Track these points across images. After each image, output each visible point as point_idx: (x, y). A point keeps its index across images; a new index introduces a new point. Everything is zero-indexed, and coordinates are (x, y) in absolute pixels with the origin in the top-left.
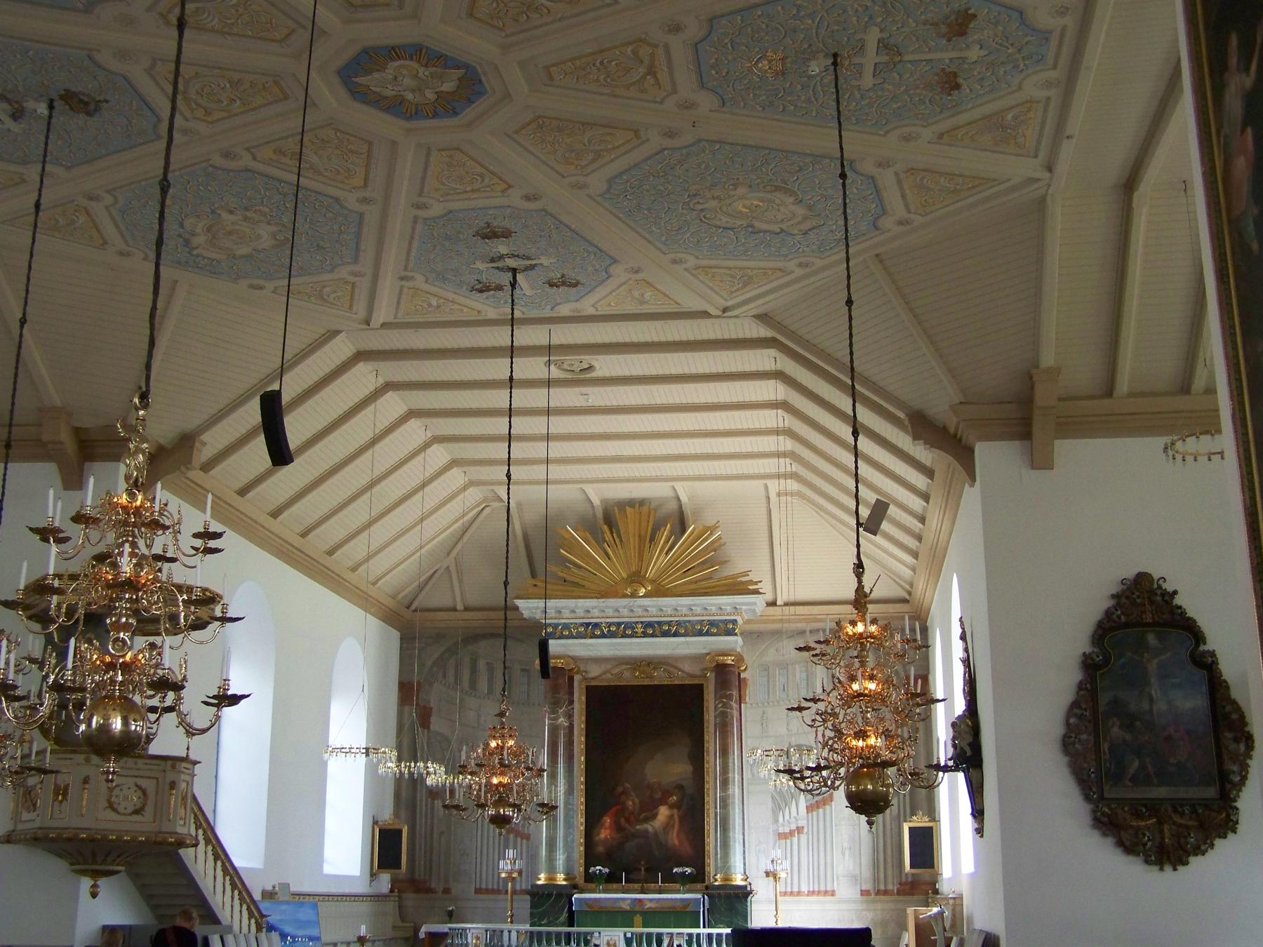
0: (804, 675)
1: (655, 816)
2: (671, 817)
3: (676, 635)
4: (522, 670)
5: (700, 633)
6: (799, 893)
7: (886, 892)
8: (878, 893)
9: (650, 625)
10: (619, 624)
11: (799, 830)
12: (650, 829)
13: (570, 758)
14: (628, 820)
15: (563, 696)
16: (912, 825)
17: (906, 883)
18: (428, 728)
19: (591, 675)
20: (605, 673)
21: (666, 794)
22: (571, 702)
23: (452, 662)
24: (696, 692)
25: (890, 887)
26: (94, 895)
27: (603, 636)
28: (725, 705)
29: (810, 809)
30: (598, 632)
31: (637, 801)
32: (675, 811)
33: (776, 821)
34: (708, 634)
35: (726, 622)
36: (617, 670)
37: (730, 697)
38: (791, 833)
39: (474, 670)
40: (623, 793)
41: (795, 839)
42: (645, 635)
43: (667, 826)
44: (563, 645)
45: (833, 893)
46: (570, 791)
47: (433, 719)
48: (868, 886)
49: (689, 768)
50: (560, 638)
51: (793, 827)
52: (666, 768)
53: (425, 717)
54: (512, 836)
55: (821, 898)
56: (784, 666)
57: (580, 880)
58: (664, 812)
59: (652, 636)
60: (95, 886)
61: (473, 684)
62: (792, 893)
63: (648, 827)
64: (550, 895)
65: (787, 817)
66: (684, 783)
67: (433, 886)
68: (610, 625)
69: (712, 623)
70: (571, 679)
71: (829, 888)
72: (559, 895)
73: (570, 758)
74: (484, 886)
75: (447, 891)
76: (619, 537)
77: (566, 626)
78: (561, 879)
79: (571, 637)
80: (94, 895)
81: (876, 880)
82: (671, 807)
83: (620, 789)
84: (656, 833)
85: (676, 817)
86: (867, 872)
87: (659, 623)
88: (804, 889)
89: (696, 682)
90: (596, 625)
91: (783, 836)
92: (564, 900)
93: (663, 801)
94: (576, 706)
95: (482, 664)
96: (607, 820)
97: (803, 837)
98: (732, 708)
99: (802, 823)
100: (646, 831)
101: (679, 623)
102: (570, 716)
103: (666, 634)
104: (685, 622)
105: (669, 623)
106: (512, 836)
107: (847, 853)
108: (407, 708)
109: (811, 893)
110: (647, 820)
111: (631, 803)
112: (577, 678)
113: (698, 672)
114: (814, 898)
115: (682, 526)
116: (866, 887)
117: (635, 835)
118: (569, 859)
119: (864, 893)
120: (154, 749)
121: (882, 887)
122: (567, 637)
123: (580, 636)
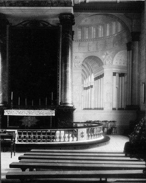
6: (91, 109)
11: (92, 86)
20: (19, 24)
25: (123, 107)
29: (96, 79)
33: (83, 83)
36: (24, 23)
38: (88, 88)
41: (90, 90)
45: (102, 109)
51: (89, 86)
56: (88, 27)
62: (88, 109)
65: (87, 82)
71: (101, 107)
81: (118, 104)
97: (93, 89)
98: (69, 37)
109: (95, 109)
112: (8, 26)
116: (115, 106)
121: (120, 107)
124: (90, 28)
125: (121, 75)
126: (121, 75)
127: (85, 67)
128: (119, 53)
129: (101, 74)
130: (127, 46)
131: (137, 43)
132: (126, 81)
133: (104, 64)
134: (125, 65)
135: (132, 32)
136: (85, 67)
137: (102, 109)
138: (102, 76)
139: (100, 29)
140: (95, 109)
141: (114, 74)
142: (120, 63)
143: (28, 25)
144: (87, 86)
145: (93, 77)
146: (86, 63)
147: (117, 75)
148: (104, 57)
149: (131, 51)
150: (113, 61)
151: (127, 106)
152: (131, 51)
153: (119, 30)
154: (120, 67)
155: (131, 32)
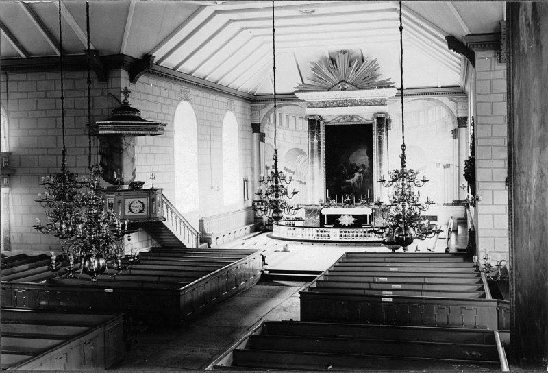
13: (319, 153)
19: (326, 121)
22: (319, 132)
24: (367, 129)
26: (129, 240)
28: (381, 134)
37: (382, 131)
47: (266, 138)
52: (360, 158)
58: (357, 175)
60: (129, 236)
63: (351, 181)
66: (365, 163)
70: (319, 123)
73: (319, 153)
76: (336, 65)
80: (129, 240)
82: (360, 173)
84: (354, 184)
89: (369, 123)
94: (321, 133)
95: (284, 116)
102: (319, 137)
110: (350, 178)
112: (321, 122)
113: (370, 119)
115: (363, 61)
120: (144, 187)
126: (447, 166)
135: (458, 118)
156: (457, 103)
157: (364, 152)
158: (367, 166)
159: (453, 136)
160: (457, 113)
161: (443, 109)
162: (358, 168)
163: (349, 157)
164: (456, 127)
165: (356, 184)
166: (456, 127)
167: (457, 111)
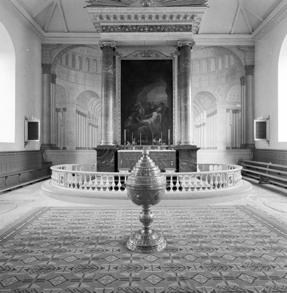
0: (206, 64)
1: (151, 116)
2: (158, 116)
3: (163, 31)
4: (94, 60)
5: (175, 31)
7: (236, 148)
8: (233, 148)
9: (152, 26)
10: (137, 26)
11: (204, 124)
12: (149, 122)
14: (140, 118)
15: (111, 59)
16: (257, 121)
17: (243, 145)
18: (55, 83)
19: (123, 56)
20: (129, 55)
21: (156, 107)
22: (114, 67)
23: (65, 55)
25: (237, 146)
27: (129, 31)
29: (208, 116)
30: (127, 30)
31: (144, 110)
32: (160, 114)
34: (179, 31)
35: (187, 26)
38: (201, 125)
39: (74, 60)
40: (136, 107)
41: (202, 128)
42: (149, 31)
43: (157, 120)
44: (110, 36)
45: (216, 148)
46: (115, 105)
47: (57, 79)
48: (229, 146)
49: (167, 96)
50: (109, 32)
52: (158, 96)
53: (53, 79)
54: (90, 127)
55: (212, 150)
57: (119, 144)
58: (155, 114)
59: (152, 31)
61: (74, 66)
63: (149, 121)
64: (106, 150)
66: (164, 102)
67: (59, 147)
68: (132, 26)
69: (180, 26)
70: (114, 57)
71: (215, 146)
72: (110, 150)
74: (80, 146)
75: (64, 148)
77: (112, 27)
78: (111, 144)
79: (114, 31)
81: (232, 143)
82: (158, 112)
83: (136, 105)
84: (152, 124)
85: (160, 117)
86: (229, 140)
87: (156, 26)
88: (205, 147)
89: (170, 59)
90: (126, 26)
91: (197, 126)
92: (113, 153)
93: (154, 110)
95: (77, 58)
96: (131, 118)
97: (205, 127)
99: (204, 122)
100: (148, 123)
101: (165, 26)
103: (159, 31)
104: (168, 26)
105: (161, 26)
106: (90, 127)
107: (222, 133)
108: (45, 75)
109: (208, 148)
110: (147, 118)
111: (141, 110)
112: (117, 57)
113: (170, 55)
114: (209, 150)
117: (143, 124)
118: (114, 134)
119: (227, 148)
122: (113, 32)
123: (118, 31)
124: (201, 61)
125: (235, 111)
126: (235, 111)
127: (197, 104)
128: (232, 88)
129: (214, 111)
130: (241, 80)
131: (250, 77)
132: (240, 117)
133: (217, 99)
134: (240, 101)
135: (246, 66)
136: (197, 104)
137: (216, 148)
138: (215, 113)
139: (213, 61)
140: (208, 148)
141: (228, 110)
142: (233, 99)
143: (139, 55)
144: (199, 124)
145: (205, 114)
146: (199, 100)
147: (231, 111)
148: (216, 92)
149: (245, 86)
150: (226, 96)
151: (241, 145)
152: (245, 86)
153: (232, 64)
154: (236, 103)
155: (244, 65)
156: (245, 52)
157: (163, 88)
158: (167, 105)
159: (241, 83)
160: (245, 61)
161: (232, 57)
162: (156, 107)
163: (146, 95)
164: (245, 75)
165: (154, 125)
166: (245, 75)
167: (245, 59)
